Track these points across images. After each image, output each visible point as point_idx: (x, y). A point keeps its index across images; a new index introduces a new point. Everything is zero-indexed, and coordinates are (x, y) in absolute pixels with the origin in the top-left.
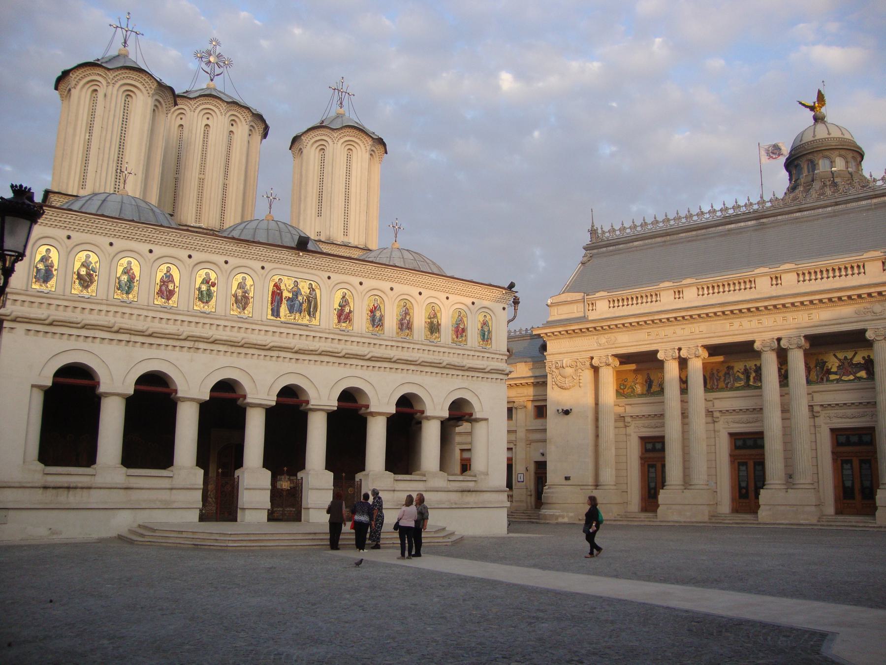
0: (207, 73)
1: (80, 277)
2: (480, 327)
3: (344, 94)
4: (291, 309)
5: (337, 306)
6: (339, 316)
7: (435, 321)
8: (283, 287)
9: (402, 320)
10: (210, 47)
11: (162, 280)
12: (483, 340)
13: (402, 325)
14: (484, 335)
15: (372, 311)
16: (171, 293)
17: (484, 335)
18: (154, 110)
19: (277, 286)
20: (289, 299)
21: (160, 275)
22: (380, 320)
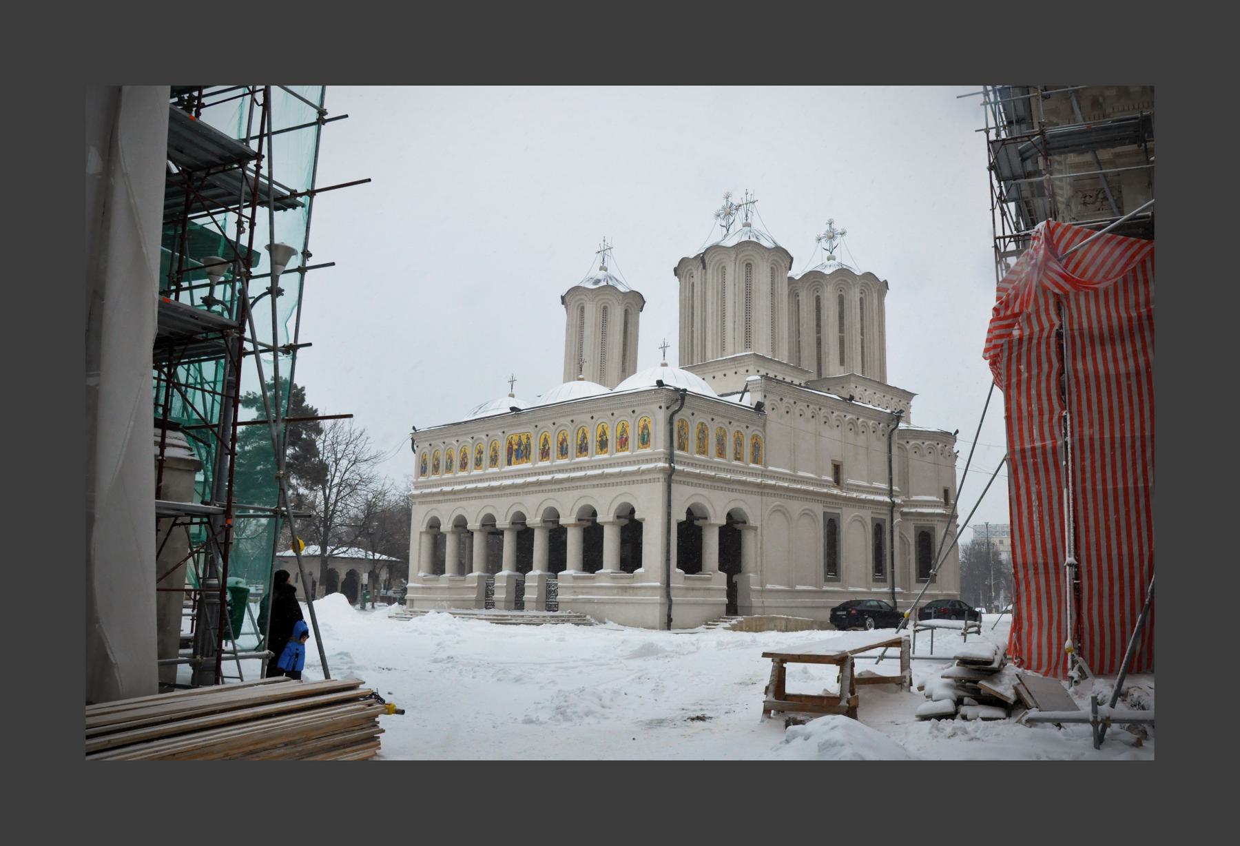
0: (724, 226)
1: (434, 465)
2: (640, 433)
3: (748, 205)
4: (517, 457)
5: (542, 447)
6: (542, 454)
7: (604, 439)
8: (513, 443)
9: (581, 445)
10: (724, 203)
11: (463, 459)
12: (643, 444)
13: (581, 448)
14: (643, 439)
15: (561, 444)
16: (466, 464)
17: (643, 439)
18: (605, 308)
19: (510, 443)
20: (517, 450)
21: (462, 454)
22: (567, 449)
